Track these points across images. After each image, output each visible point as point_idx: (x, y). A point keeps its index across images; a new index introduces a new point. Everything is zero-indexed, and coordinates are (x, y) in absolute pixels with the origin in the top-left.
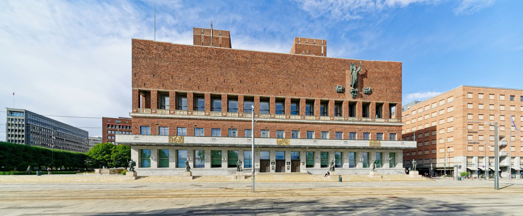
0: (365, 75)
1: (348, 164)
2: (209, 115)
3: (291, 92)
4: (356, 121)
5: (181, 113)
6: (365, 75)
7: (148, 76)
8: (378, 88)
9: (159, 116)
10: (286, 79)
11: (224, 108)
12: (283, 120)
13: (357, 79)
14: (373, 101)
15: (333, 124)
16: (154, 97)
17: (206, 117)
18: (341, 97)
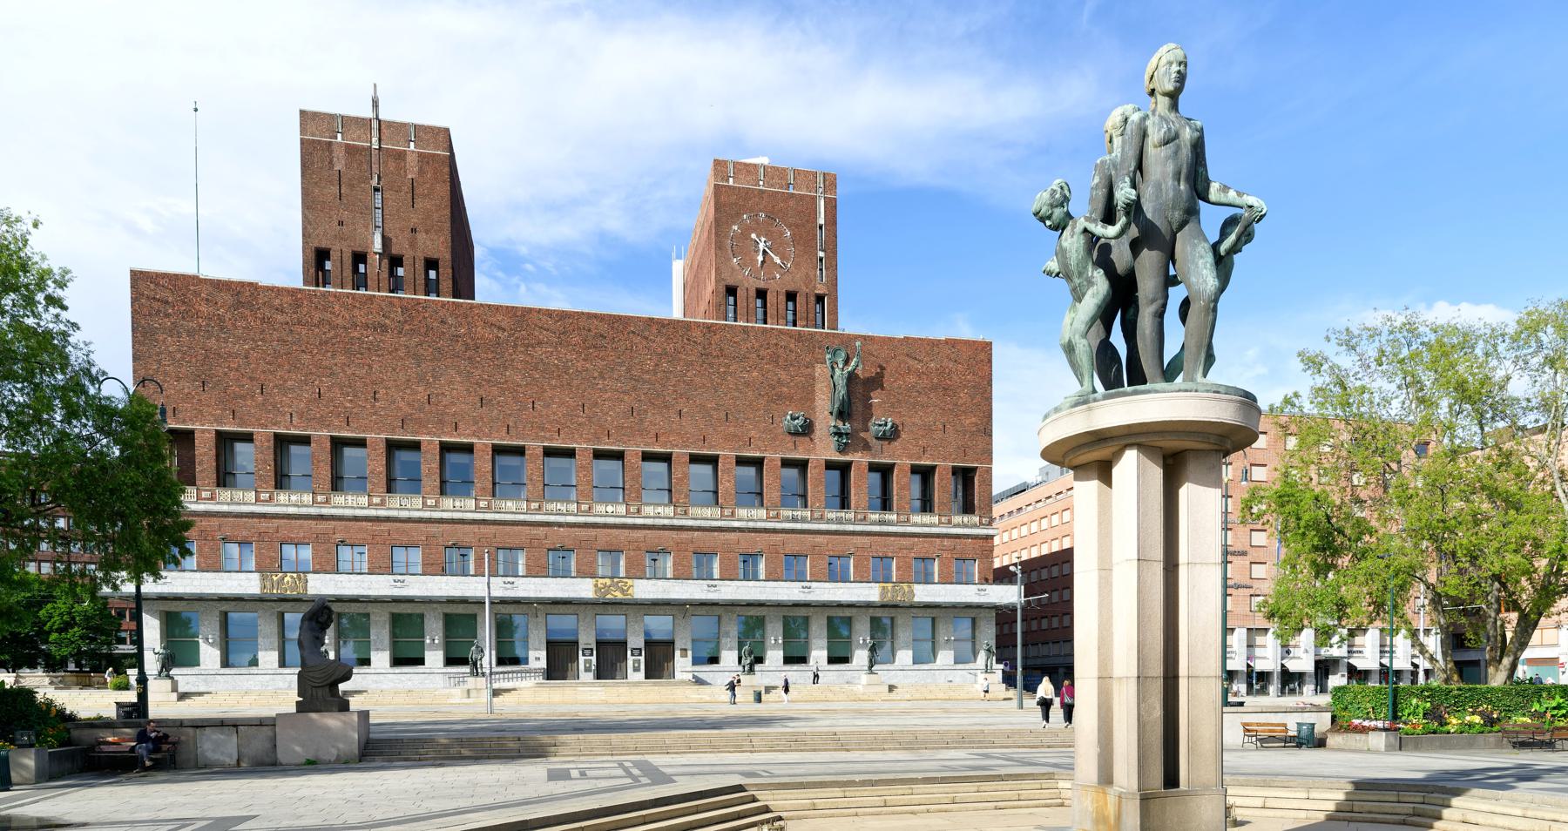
0: (876, 382)
1: (825, 653)
2: (383, 503)
4: (849, 522)
5: (294, 498)
6: (876, 382)
7: (186, 386)
13: (849, 392)
14: (901, 457)
15: (775, 531)
17: (372, 513)
18: (800, 449)
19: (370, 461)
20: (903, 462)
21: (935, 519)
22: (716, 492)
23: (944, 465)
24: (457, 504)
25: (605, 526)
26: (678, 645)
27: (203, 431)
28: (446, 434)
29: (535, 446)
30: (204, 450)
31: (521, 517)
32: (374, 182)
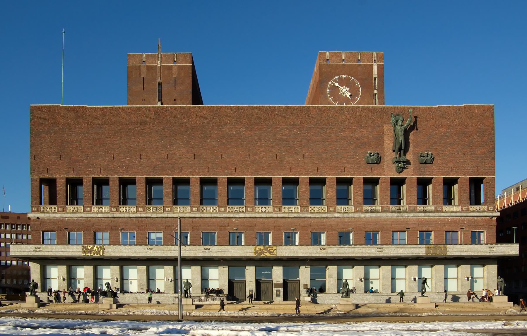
10: (272, 147)
11: (168, 198)
16: (60, 187)
19: (138, 191)
24: (182, 209)
27: (60, 179)
28: (175, 174)
29: (222, 178)
31: (215, 215)
32: (158, 81)
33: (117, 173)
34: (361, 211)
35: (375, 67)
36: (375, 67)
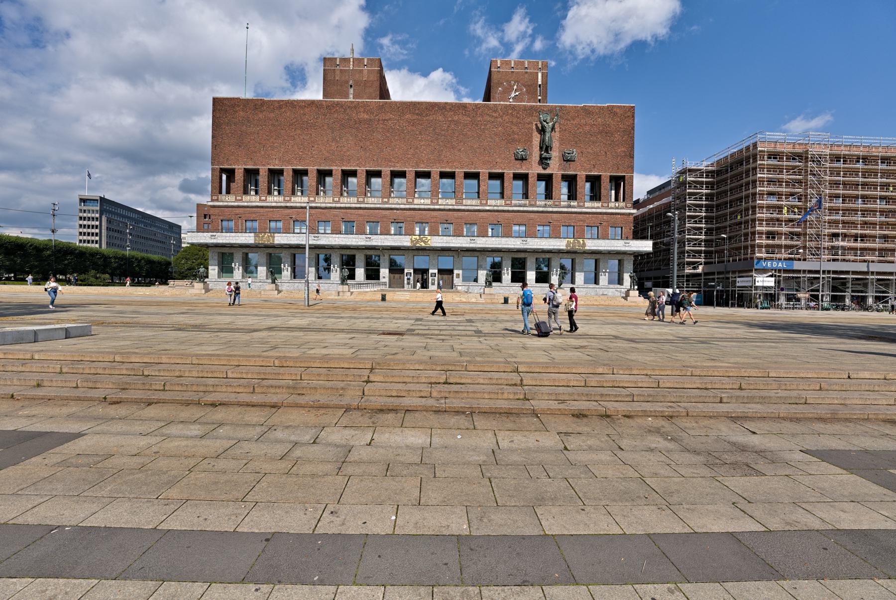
3: (440, 161)
4: (550, 206)
8: (590, 150)
9: (246, 204)
12: (426, 207)
15: (508, 211)
20: (582, 174)
21: (599, 204)
22: (478, 193)
23: (605, 175)
25: (420, 210)
26: (456, 272)
30: (239, 176)
31: (378, 206)
33: (291, 164)
34: (510, 205)
35: (540, 75)
36: (540, 75)
